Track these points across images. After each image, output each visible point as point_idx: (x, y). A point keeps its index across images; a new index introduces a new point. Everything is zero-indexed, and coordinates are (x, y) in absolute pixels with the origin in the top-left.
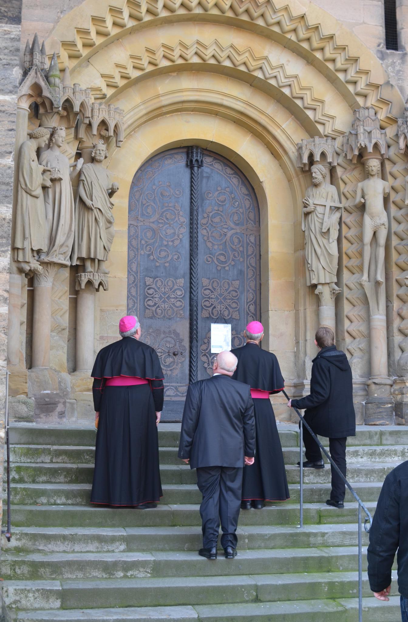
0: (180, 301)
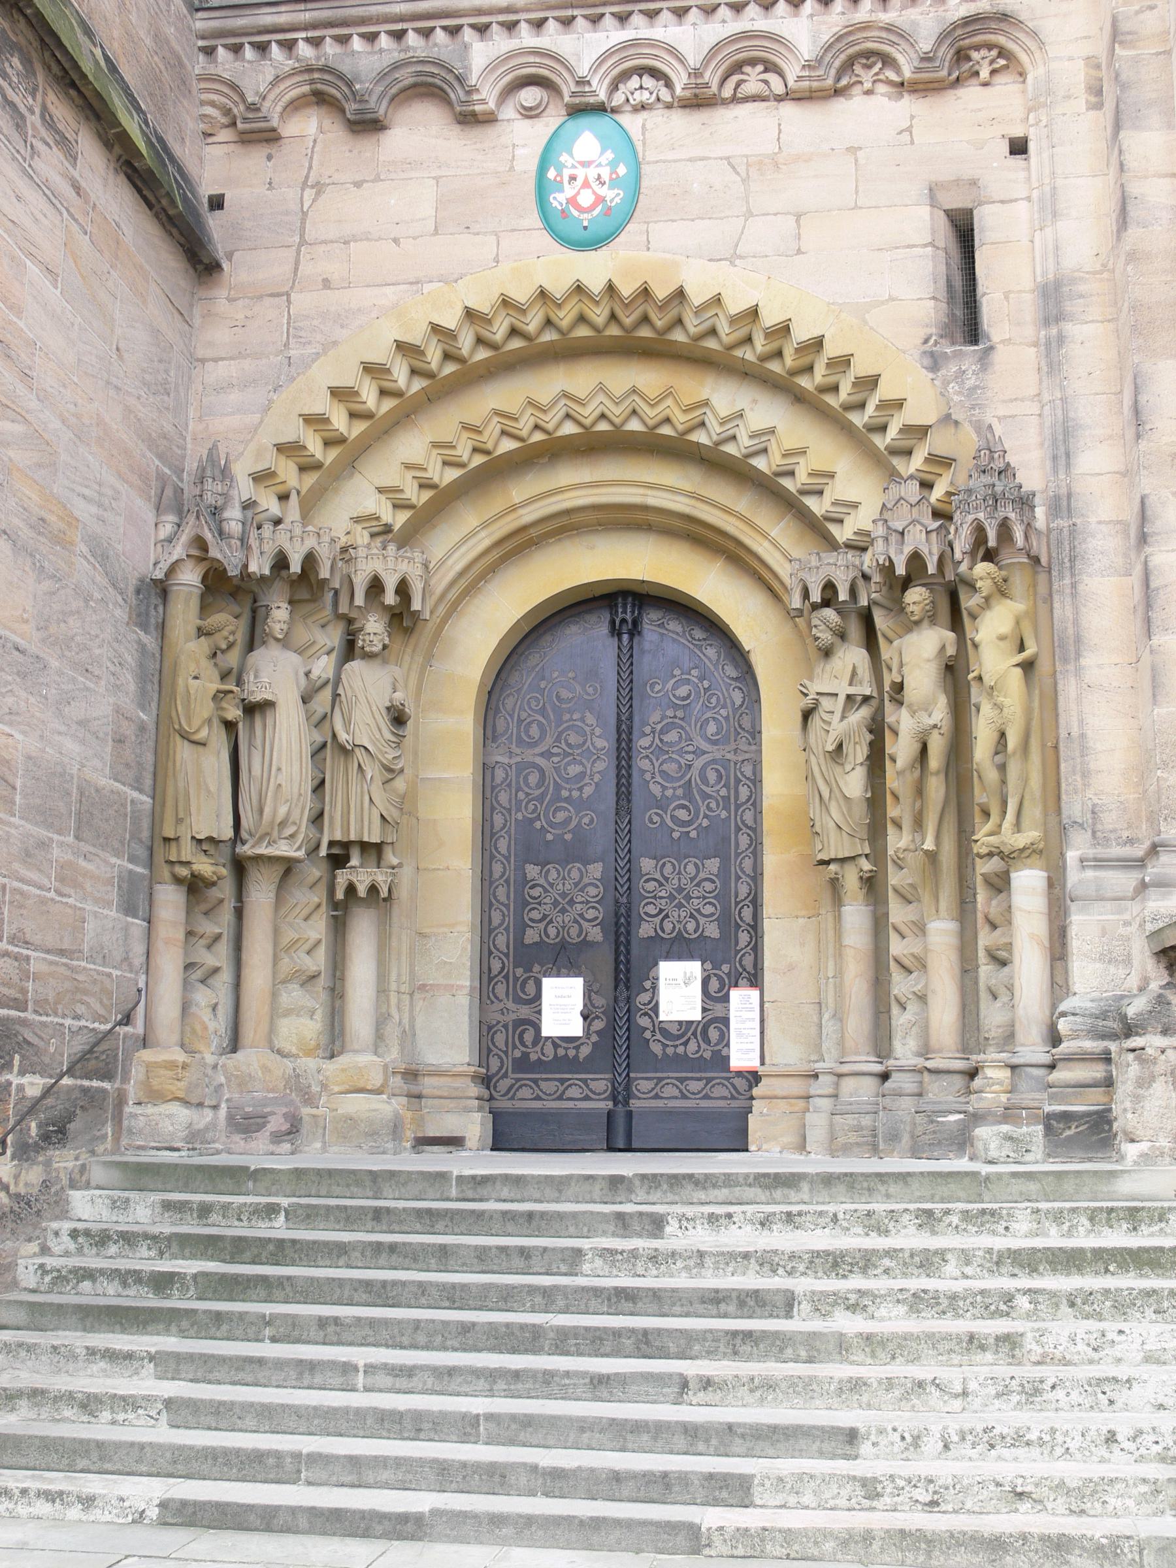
0: (593, 907)
